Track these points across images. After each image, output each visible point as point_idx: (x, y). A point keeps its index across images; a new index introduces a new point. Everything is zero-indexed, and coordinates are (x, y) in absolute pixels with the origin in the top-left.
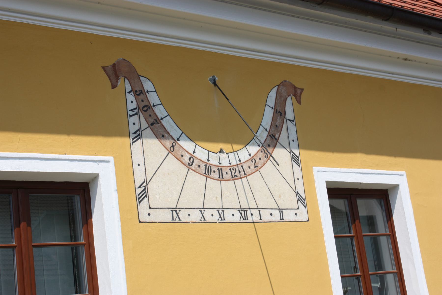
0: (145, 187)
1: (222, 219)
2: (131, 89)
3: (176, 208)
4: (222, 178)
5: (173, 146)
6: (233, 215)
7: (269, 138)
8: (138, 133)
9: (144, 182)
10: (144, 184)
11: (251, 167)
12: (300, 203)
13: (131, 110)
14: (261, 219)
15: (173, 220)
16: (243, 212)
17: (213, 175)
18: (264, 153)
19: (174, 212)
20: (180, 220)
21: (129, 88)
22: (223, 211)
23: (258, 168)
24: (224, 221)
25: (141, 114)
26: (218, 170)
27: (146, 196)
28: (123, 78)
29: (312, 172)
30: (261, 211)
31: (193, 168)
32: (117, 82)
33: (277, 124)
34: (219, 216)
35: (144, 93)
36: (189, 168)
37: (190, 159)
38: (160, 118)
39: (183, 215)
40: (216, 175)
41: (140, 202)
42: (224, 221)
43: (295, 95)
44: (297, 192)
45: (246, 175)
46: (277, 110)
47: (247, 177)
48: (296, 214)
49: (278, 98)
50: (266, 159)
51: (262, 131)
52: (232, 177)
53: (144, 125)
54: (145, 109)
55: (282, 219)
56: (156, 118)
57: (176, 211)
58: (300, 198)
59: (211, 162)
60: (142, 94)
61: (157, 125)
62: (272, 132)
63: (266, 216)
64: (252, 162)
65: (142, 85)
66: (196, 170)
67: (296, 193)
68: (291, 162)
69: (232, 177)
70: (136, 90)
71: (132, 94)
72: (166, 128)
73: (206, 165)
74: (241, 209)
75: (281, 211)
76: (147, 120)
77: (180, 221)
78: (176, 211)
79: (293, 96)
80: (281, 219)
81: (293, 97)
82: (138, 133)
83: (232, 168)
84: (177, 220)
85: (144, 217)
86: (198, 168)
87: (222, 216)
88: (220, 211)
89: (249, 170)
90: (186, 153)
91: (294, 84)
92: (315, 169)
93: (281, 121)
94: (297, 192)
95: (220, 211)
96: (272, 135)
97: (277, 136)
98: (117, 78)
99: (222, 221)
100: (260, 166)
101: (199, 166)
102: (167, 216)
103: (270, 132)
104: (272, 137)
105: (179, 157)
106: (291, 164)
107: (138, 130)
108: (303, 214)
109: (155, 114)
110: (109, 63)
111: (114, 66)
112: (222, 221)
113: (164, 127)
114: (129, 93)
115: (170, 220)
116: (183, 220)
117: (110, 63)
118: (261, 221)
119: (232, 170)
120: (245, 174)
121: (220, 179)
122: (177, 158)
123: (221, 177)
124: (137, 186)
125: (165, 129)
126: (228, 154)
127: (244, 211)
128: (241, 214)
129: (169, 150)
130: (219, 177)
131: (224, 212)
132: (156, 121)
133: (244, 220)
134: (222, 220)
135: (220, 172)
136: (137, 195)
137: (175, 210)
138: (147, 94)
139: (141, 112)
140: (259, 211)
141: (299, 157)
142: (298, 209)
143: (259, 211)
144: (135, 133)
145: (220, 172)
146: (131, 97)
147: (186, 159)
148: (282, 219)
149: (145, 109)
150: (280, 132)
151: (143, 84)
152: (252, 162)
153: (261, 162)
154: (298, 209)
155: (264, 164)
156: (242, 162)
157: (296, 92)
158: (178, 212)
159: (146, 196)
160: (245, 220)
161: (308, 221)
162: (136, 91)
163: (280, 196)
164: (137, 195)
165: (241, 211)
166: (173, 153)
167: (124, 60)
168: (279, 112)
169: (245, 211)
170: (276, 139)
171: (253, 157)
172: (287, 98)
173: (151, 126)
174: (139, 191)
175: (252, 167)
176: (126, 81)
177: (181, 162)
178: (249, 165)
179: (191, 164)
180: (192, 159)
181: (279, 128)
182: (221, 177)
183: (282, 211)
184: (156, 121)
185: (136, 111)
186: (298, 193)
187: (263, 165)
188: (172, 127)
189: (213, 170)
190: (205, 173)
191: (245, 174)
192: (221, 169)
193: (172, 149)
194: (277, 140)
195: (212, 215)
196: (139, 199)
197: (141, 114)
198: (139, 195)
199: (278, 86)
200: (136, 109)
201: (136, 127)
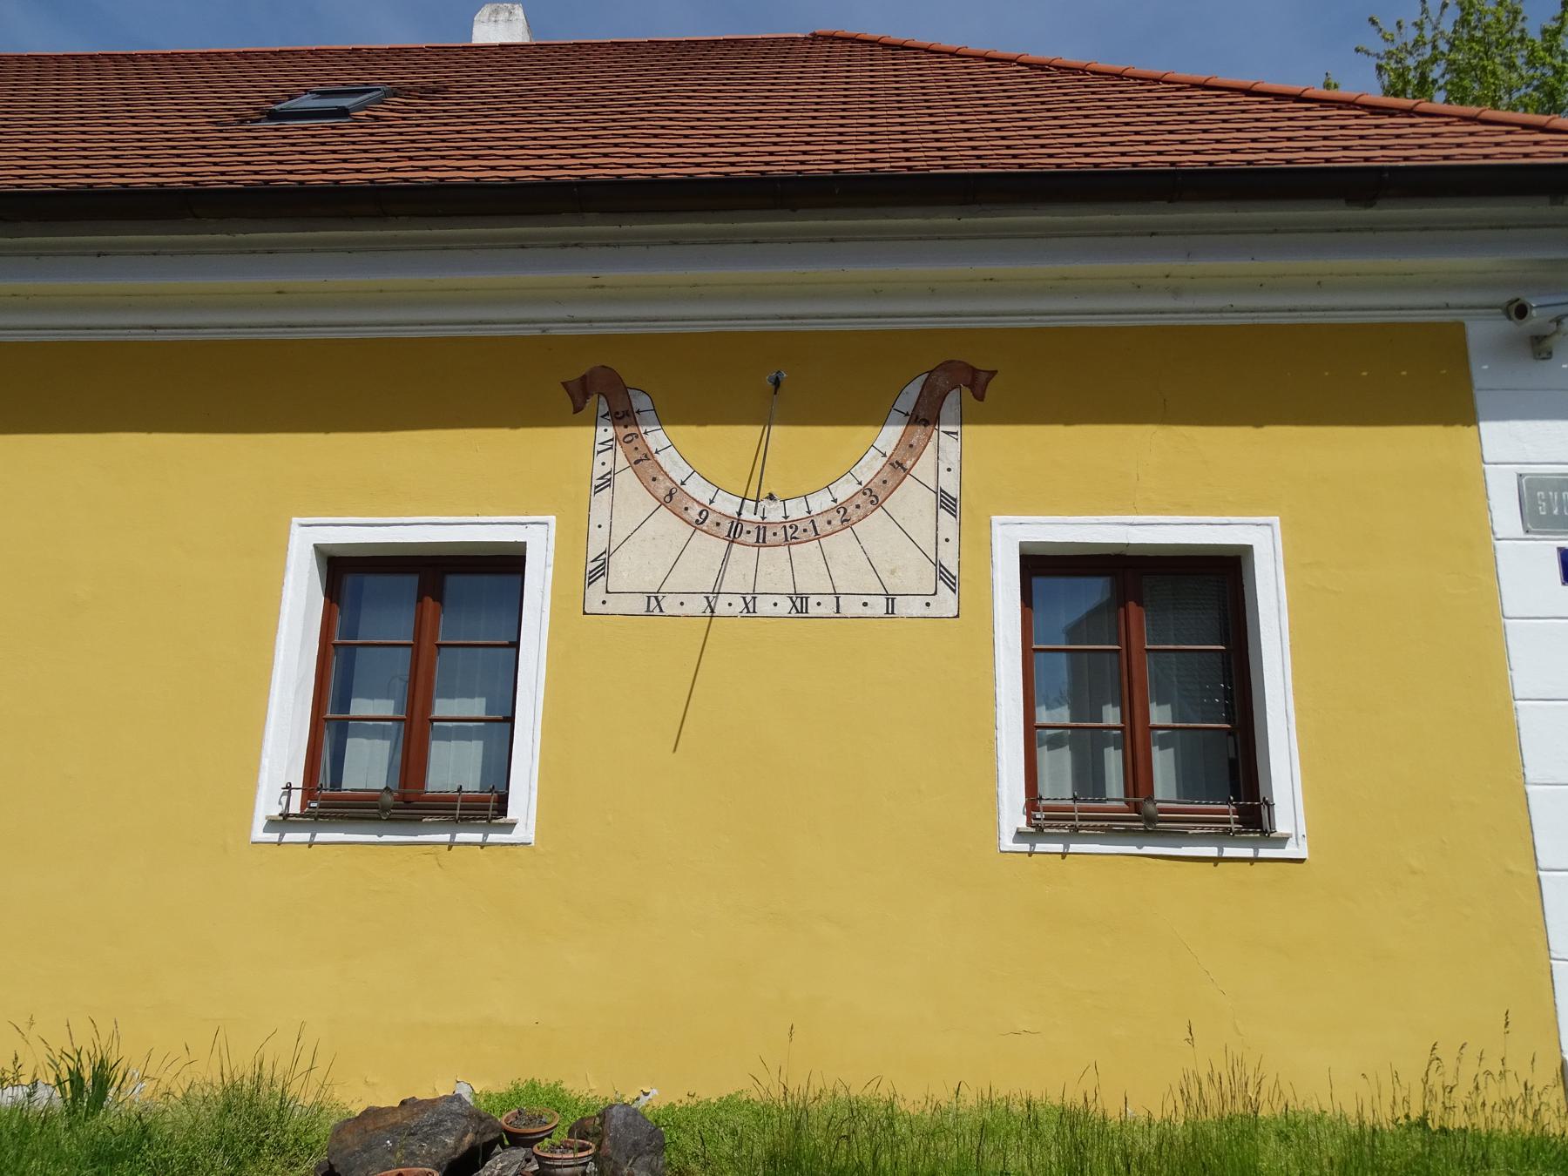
0: (605, 559)
1: (750, 610)
2: (607, 410)
3: (658, 593)
4: (764, 541)
5: (671, 495)
6: (775, 604)
7: (889, 468)
8: (608, 477)
9: (605, 552)
10: (604, 556)
11: (833, 522)
12: (943, 584)
13: (602, 444)
14: (838, 612)
15: (648, 610)
16: (799, 599)
17: (744, 537)
18: (871, 496)
19: (653, 599)
20: (661, 611)
22: (754, 598)
23: (850, 523)
24: (754, 615)
25: (618, 447)
26: (756, 530)
27: (603, 574)
28: (596, 396)
29: (290, 522)
30: (842, 598)
31: (705, 528)
32: (585, 402)
33: (914, 441)
34: (792, 605)
35: (631, 414)
36: (696, 528)
37: (701, 513)
38: (654, 452)
39: (669, 605)
40: (752, 539)
41: (590, 584)
42: (754, 615)
43: (971, 386)
44: (938, 565)
46: (917, 418)
47: (821, 540)
48: (928, 604)
49: (925, 394)
50: (871, 507)
51: (874, 457)
52: (786, 540)
53: (622, 461)
54: (630, 438)
55: (890, 611)
56: (647, 451)
57: (656, 598)
58: (942, 573)
59: (793, 516)
60: (626, 417)
61: (646, 463)
62: (895, 458)
63: (851, 606)
64: (839, 512)
65: (630, 401)
66: (710, 532)
67: (936, 565)
68: (935, 508)
69: (786, 540)
70: (618, 410)
71: (609, 418)
72: (662, 465)
73: (733, 522)
74: (795, 594)
75: (890, 598)
76: (629, 456)
77: (661, 614)
78: (656, 598)
79: (966, 386)
80: (888, 613)
81: (967, 391)
82: (608, 477)
83: (788, 525)
84: (657, 611)
85: (594, 605)
86: (715, 528)
87: (751, 606)
88: (749, 598)
89: (829, 527)
90: (695, 503)
91: (971, 364)
93: (926, 435)
94: (938, 565)
95: (749, 598)
96: (897, 462)
97: (908, 464)
98: (586, 396)
99: (749, 615)
100: (854, 519)
101: (718, 524)
102: (639, 605)
103: (894, 456)
104: (897, 466)
105: (680, 510)
106: (935, 513)
107: (610, 473)
108: (947, 601)
109: (647, 446)
110: (574, 375)
111: (584, 377)
112: (749, 615)
113: (660, 465)
114: (602, 417)
115: (643, 610)
116: (667, 611)
117: (576, 375)
118: (838, 615)
119: (788, 528)
120: (817, 534)
121: (757, 544)
122: (674, 513)
123: (761, 541)
124: (591, 558)
125: (661, 468)
126: (784, 501)
127: (802, 598)
128: (794, 603)
129: (662, 500)
130: (758, 541)
131: (756, 600)
132: (646, 456)
133: (798, 612)
134: (749, 612)
135: (762, 532)
136: (588, 572)
137: (655, 597)
138: (637, 415)
139: (620, 444)
140: (838, 598)
141: (958, 499)
142: (585, 613)
143: (838, 598)
144: (602, 478)
145: (762, 532)
147: (694, 513)
148: (890, 611)
149: (630, 438)
150: (913, 460)
151: (633, 400)
152: (839, 512)
153: (860, 512)
154: (585, 613)
155: (867, 516)
156: (812, 513)
157: (974, 379)
158: (660, 598)
159: (603, 574)
160: (802, 612)
161: (958, 616)
162: (617, 413)
163: (893, 572)
164: (588, 572)
165: (794, 599)
166: (668, 505)
167: (603, 366)
168: (924, 420)
169: (804, 598)
170: (905, 470)
171: (841, 504)
172: (948, 393)
173: (634, 465)
174: (591, 567)
175: (836, 522)
176: (602, 399)
177: (681, 518)
178: (829, 519)
179: (701, 520)
180: (704, 513)
181: (916, 448)
182: (761, 541)
183: (893, 599)
184: (646, 456)
185: (611, 443)
186: (941, 565)
187: (864, 518)
188: (675, 463)
189: (745, 529)
190: (729, 536)
191: (817, 534)
192: (765, 528)
193: (668, 499)
194: (907, 472)
195: (730, 604)
196: (590, 578)
197: (618, 447)
198: (590, 572)
199: (930, 372)
200: (612, 440)
201: (607, 469)
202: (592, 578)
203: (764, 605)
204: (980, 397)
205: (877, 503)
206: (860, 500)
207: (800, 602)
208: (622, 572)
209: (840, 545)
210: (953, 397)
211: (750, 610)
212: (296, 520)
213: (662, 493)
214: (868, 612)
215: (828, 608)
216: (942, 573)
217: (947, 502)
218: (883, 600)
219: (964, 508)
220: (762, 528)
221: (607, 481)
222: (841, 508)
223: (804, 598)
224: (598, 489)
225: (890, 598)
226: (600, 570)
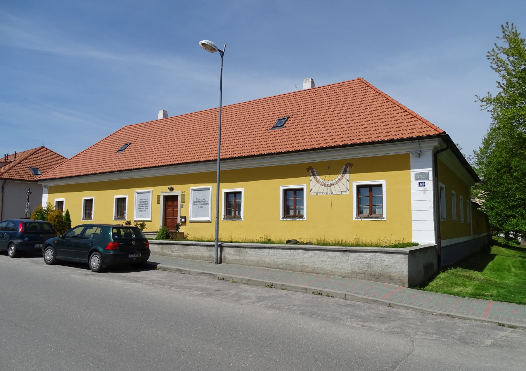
1: (327, 194)
7: (341, 177)
17: (326, 186)
21: (311, 171)
40: (327, 186)
44: (347, 188)
45: (334, 185)
55: (342, 194)
58: (347, 189)
63: (338, 193)
75: (342, 192)
85: (311, 194)
92: (353, 182)
94: (347, 188)
108: (348, 192)
115: (316, 194)
117: (307, 168)
137: (317, 193)
146: (311, 173)
147: (321, 183)
148: (342, 194)
169: (333, 192)
194: (343, 177)
202: (310, 191)
203: (328, 194)
204: (352, 167)
205: (340, 181)
206: (338, 181)
207: (332, 193)
208: (314, 190)
209: (336, 186)
210: (349, 167)
211: (327, 194)
212: (281, 186)
213: (317, 181)
214: (339, 194)
215: (335, 194)
216: (347, 189)
217: (348, 180)
218: (341, 192)
219: (350, 181)
220: (328, 184)
221: (311, 180)
222: (336, 182)
223: (333, 192)
224: (311, 181)
225: (342, 192)
226: (311, 190)
